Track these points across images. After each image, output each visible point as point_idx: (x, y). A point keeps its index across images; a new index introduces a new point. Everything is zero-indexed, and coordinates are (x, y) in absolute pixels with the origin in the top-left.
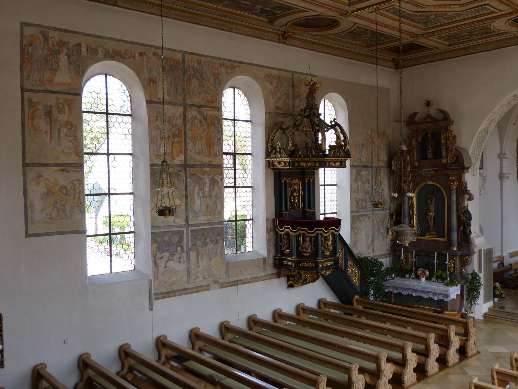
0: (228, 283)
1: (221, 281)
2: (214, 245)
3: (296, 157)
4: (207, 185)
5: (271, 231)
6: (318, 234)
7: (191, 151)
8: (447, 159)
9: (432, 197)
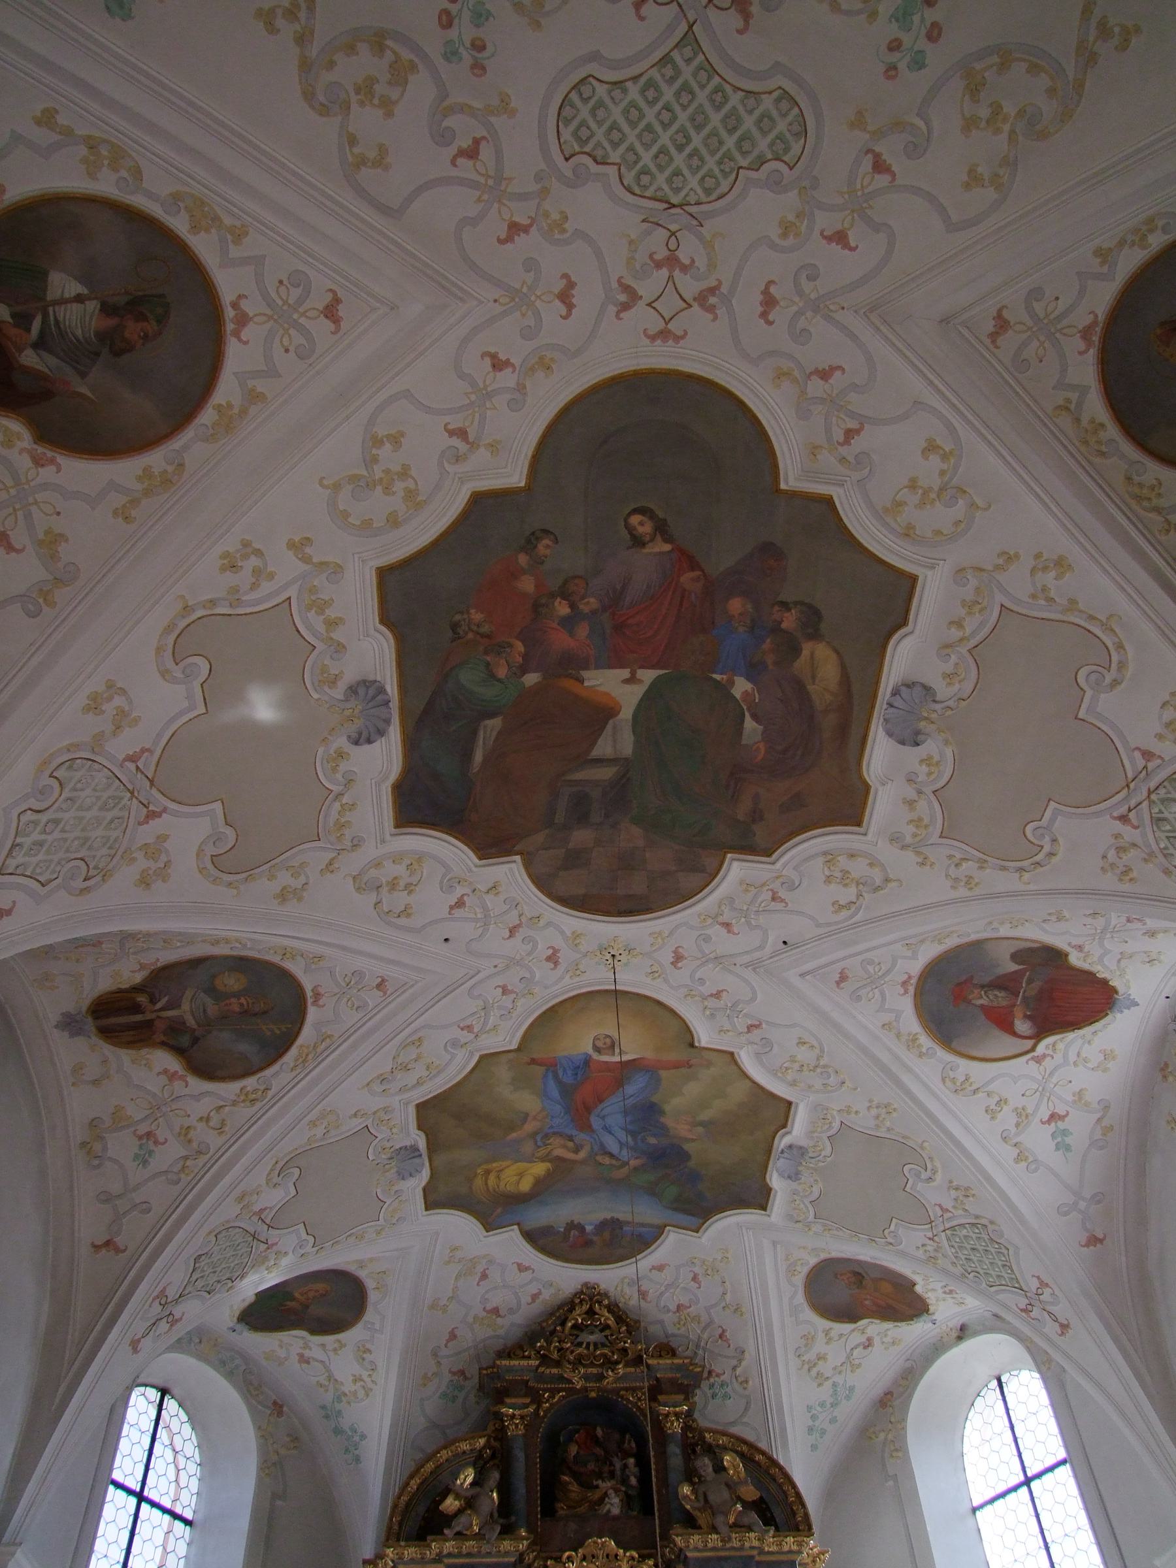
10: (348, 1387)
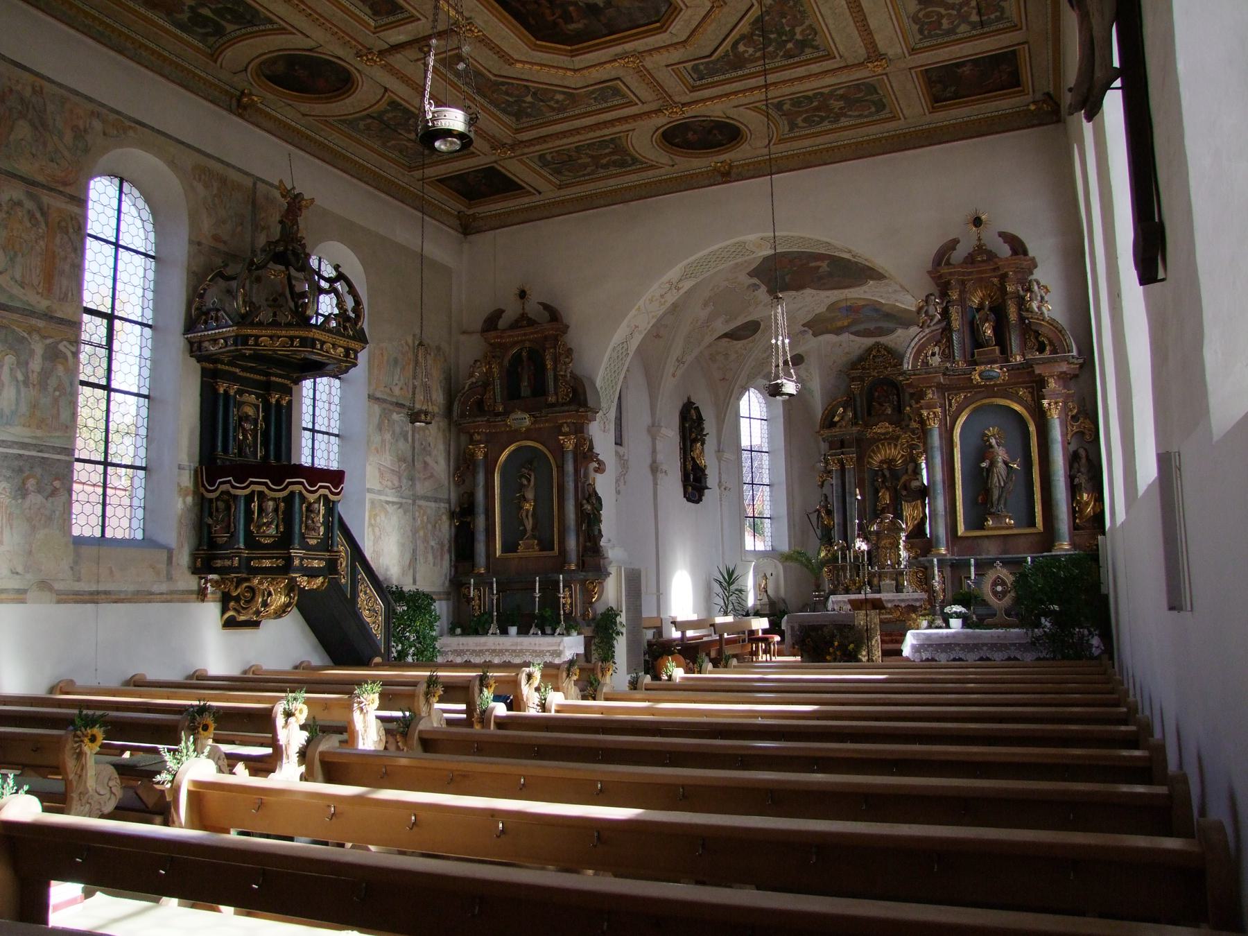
0: (77, 593)
1: (58, 586)
2: (46, 499)
3: (253, 325)
5: (186, 495)
6: (292, 493)
8: (556, 394)
9: (530, 472)
10: (805, 378)
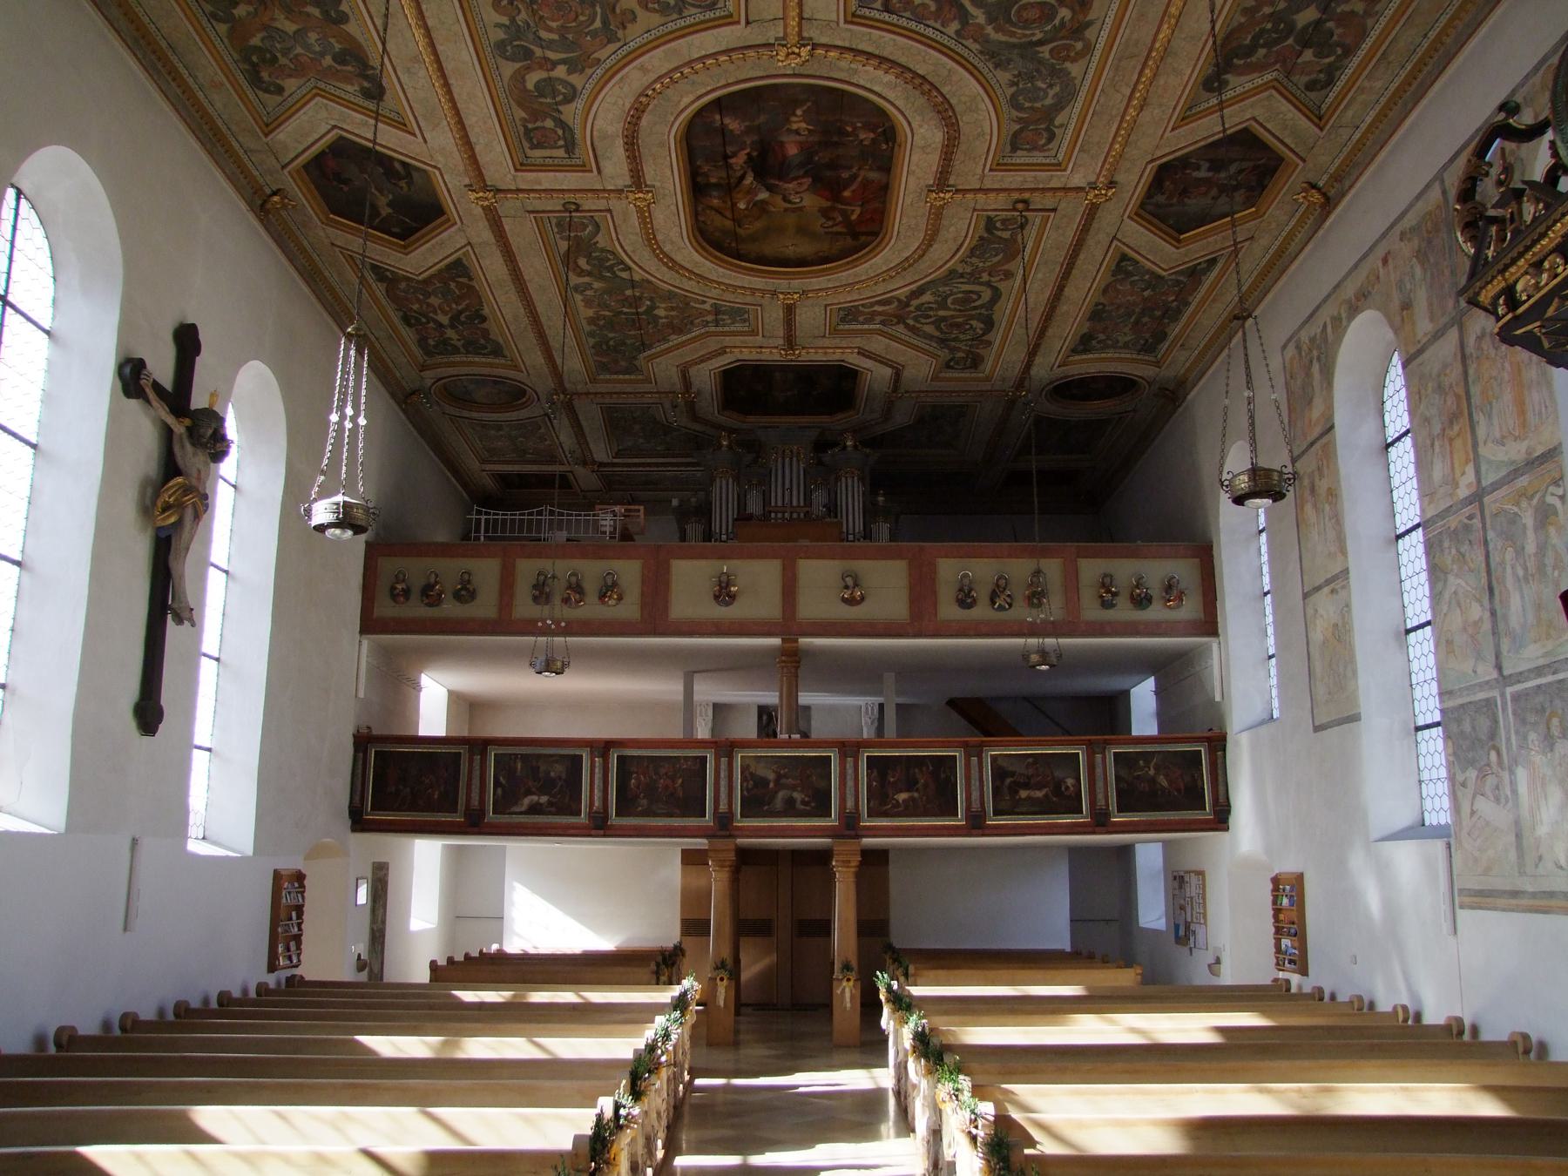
4: (1530, 534)
7: (1485, 443)
